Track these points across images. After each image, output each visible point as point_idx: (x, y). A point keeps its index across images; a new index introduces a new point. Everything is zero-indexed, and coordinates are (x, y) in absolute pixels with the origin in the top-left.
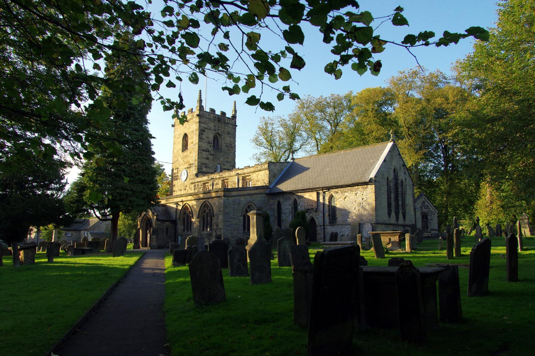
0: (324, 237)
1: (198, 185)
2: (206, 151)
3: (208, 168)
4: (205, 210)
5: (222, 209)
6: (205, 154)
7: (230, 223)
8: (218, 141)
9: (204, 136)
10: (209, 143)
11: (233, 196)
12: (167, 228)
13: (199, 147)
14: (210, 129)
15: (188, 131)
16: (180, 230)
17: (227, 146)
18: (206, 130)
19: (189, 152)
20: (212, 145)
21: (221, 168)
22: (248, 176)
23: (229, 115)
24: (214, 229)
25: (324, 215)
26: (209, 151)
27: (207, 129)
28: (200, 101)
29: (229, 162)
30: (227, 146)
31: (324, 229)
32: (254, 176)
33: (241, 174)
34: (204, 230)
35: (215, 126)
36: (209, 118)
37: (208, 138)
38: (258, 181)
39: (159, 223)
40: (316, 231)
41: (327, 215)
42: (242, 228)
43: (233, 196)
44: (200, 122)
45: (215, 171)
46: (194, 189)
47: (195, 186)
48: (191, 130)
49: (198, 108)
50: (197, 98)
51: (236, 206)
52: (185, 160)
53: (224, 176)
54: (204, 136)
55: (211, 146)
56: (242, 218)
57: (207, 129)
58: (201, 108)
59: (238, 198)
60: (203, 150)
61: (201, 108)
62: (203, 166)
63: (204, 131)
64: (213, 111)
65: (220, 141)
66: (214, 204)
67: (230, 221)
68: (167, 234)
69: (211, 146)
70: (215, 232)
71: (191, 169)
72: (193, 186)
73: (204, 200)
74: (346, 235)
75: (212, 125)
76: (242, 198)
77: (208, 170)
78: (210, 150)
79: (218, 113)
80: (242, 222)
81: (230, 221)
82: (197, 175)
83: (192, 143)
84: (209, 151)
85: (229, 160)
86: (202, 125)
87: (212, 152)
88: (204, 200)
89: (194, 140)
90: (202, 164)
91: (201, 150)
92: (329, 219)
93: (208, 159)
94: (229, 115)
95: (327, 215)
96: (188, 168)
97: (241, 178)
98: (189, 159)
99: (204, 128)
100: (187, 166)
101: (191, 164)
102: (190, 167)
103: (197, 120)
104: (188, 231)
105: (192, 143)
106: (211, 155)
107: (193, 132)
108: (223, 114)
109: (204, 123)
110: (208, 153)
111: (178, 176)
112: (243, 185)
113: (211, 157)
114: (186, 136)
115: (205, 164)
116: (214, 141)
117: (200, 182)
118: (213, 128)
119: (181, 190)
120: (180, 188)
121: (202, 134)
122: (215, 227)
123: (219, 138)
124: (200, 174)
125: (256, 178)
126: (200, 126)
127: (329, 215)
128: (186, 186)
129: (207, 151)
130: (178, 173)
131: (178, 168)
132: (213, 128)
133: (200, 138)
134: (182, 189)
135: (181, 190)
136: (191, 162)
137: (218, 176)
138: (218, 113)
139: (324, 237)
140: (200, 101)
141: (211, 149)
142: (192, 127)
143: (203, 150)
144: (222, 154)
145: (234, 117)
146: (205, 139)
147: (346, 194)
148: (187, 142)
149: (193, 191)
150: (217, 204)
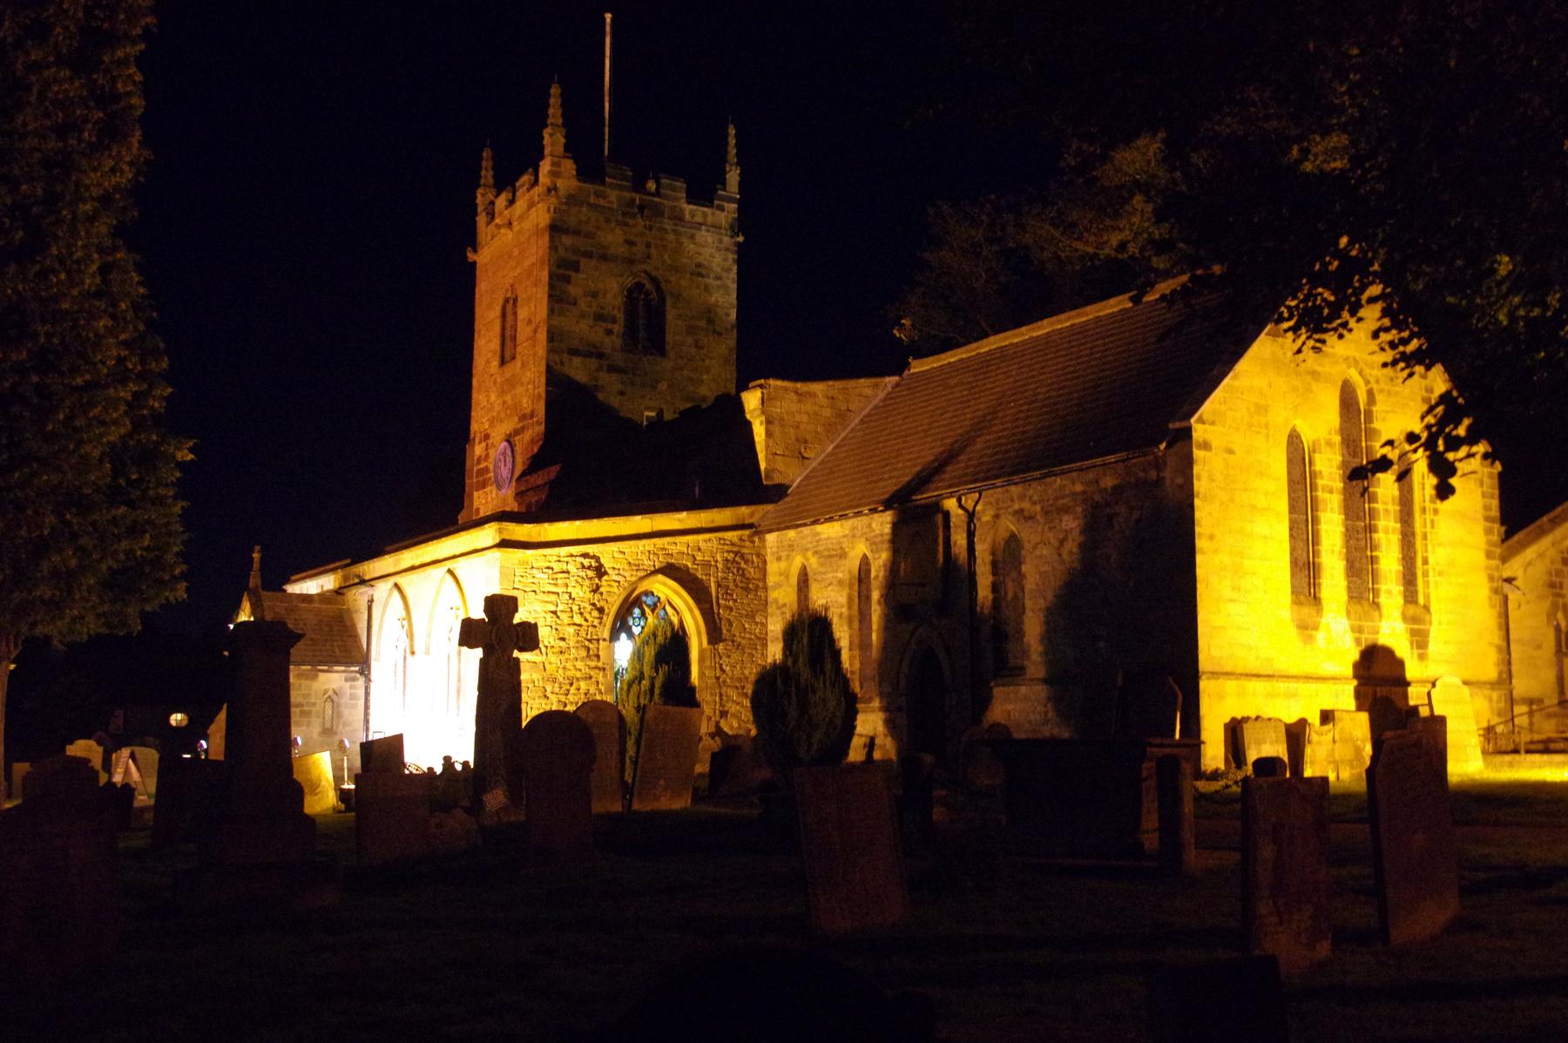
2: (588, 355)
10: (600, 317)
18: (583, 261)
26: (600, 356)
30: (691, 330)
36: (595, 207)
37: (595, 295)
54: (573, 291)
55: (609, 332)
57: (589, 255)
69: (609, 332)
84: (600, 356)
86: (567, 240)
106: (612, 369)
109: (577, 233)
110: (593, 363)
121: (568, 280)
126: (553, 247)
133: (558, 299)
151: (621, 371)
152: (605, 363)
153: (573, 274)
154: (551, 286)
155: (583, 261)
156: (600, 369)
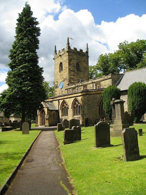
3: (75, 80)
5: (86, 102)
6: (72, 73)
8: (79, 65)
10: (74, 67)
11: (92, 94)
12: (54, 114)
13: (69, 69)
14: (74, 59)
17: (84, 68)
20: (76, 68)
21: (81, 80)
26: (74, 71)
28: (68, 44)
32: (102, 83)
33: (94, 82)
37: (73, 64)
38: (105, 85)
39: (49, 112)
42: (98, 113)
43: (92, 94)
44: (68, 55)
45: (78, 82)
49: (68, 48)
50: (67, 42)
53: (84, 84)
56: (98, 107)
57: (73, 59)
58: (69, 47)
60: (71, 71)
61: (69, 47)
63: (71, 60)
64: (75, 49)
67: (91, 109)
69: (75, 68)
71: (65, 81)
73: (75, 98)
76: (97, 96)
77: (74, 82)
79: (78, 50)
81: (91, 109)
82: (68, 85)
89: (66, 65)
90: (71, 78)
91: (70, 71)
94: (84, 51)
96: (63, 81)
97: (94, 84)
98: (63, 76)
99: (71, 58)
100: (62, 80)
101: (65, 79)
103: (67, 54)
107: (65, 61)
108: (81, 50)
110: (74, 72)
113: (75, 74)
114: (61, 63)
115: (73, 78)
116: (77, 66)
117: (71, 88)
124: (70, 84)
125: (104, 84)
126: (69, 58)
128: (63, 91)
129: (73, 71)
130: (58, 84)
131: (57, 82)
132: (76, 58)
133: (69, 64)
134: (61, 93)
135: (60, 94)
136: (65, 78)
137: (81, 84)
140: (68, 44)
141: (75, 70)
142: (65, 59)
143: (71, 71)
145: (87, 52)
148: (62, 67)
154: (69, 63)
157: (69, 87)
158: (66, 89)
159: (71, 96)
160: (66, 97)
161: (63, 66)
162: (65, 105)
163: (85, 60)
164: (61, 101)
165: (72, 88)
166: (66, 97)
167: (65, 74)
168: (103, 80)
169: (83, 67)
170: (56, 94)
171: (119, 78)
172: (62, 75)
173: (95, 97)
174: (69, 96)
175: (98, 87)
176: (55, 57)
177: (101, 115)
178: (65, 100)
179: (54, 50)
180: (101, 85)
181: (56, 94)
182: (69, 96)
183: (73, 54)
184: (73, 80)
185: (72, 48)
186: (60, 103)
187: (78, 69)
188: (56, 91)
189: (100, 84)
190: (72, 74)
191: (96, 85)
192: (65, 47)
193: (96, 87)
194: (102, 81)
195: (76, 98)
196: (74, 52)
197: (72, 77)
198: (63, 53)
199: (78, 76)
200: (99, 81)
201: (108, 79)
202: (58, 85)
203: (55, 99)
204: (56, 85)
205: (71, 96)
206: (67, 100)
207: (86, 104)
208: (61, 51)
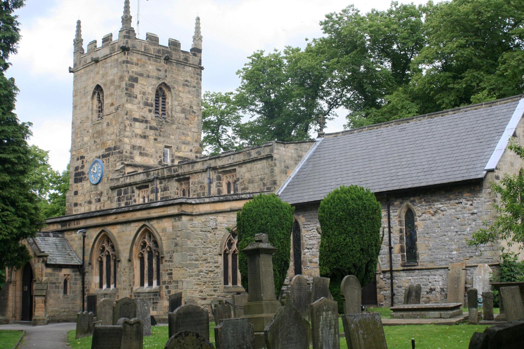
0: (393, 295)
1: (126, 193)
2: (142, 122)
3: (146, 155)
4: (145, 243)
7: (196, 270)
8: (164, 98)
9: (137, 89)
10: (146, 104)
12: (66, 282)
14: (148, 76)
15: (103, 81)
16: (93, 286)
17: (183, 111)
18: (140, 78)
19: (105, 124)
20: (153, 108)
21: (172, 156)
22: (230, 171)
23: (186, 46)
24: (164, 283)
25: (391, 248)
26: (146, 122)
27: (141, 75)
28: (127, 19)
29: (188, 143)
31: (392, 278)
32: (243, 172)
33: (214, 169)
34: (142, 284)
35: (160, 71)
37: (144, 93)
38: (251, 181)
39: (49, 270)
40: (375, 283)
41: (396, 248)
42: (222, 279)
46: (119, 200)
47: (119, 194)
48: (111, 78)
51: (209, 235)
52: (98, 140)
55: (150, 111)
56: (221, 259)
57: (141, 75)
59: (211, 217)
60: (135, 120)
61: (128, 32)
62: (136, 153)
63: (136, 80)
64: (152, 39)
65: (169, 100)
66: (164, 230)
67: (196, 266)
68: (65, 292)
70: (167, 287)
71: (112, 159)
72: (115, 193)
73: (141, 224)
74: (438, 289)
75: (151, 67)
76: (220, 218)
78: (149, 119)
79: (164, 42)
80: (222, 267)
83: (112, 104)
84: (146, 122)
85: (189, 139)
87: (154, 124)
88: (141, 224)
92: (403, 256)
93: (145, 137)
94: (186, 46)
95: (396, 248)
96: (104, 156)
98: (105, 137)
100: (101, 152)
101: (109, 149)
102: (108, 155)
104: (109, 286)
105: (112, 104)
106: (151, 128)
107: (112, 82)
108: (175, 44)
110: (144, 125)
111: (83, 173)
112: (219, 191)
115: (140, 147)
116: (157, 101)
117: (130, 185)
118: (155, 74)
119: (90, 202)
120: (88, 199)
121: (132, 86)
122: (165, 278)
123: (167, 93)
125: (247, 176)
127: (402, 250)
130: (83, 167)
131: (82, 157)
132: (155, 74)
134: (93, 201)
138: (164, 42)
139: (393, 295)
140: (127, 19)
141: (150, 116)
143: (135, 120)
144: (174, 126)
145: (196, 51)
146: (139, 96)
147: (438, 205)
149: (115, 205)
150: (170, 229)
151: (156, 129)
152: (149, 125)
153: (135, 84)
155: (140, 78)
156: (146, 128)
157: (121, 182)
158: (113, 189)
159: (129, 216)
160: (110, 219)
161: (107, 101)
162: (108, 248)
163: (189, 79)
164: (93, 234)
165: (135, 184)
166: (110, 219)
167: (111, 130)
168: (245, 163)
169: (179, 105)
170: (76, 205)
171: (300, 157)
172: (100, 133)
173: (212, 224)
174: (121, 218)
175: (229, 184)
176: (75, 65)
177: (230, 284)
178: (109, 229)
179: (74, 37)
180: (238, 179)
181: (76, 205)
182: (121, 218)
183: (144, 59)
184: (141, 154)
185: (141, 35)
186: (90, 242)
187: (161, 112)
188: (76, 193)
189: (234, 174)
190: (139, 131)
191: (219, 179)
192: (115, 29)
193: (219, 185)
194: (241, 164)
195: (147, 223)
196: (145, 53)
197: (139, 142)
198: (106, 51)
199: (160, 139)
200: (231, 165)
201: (261, 159)
202: (86, 170)
203: (73, 226)
204: (77, 168)
205: (129, 216)
206: (114, 231)
207: (178, 248)
208: (99, 44)
